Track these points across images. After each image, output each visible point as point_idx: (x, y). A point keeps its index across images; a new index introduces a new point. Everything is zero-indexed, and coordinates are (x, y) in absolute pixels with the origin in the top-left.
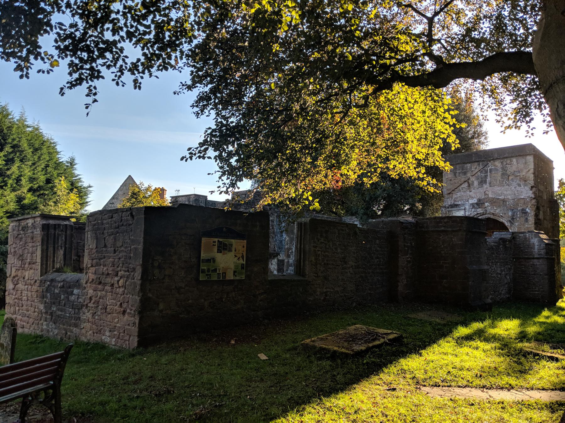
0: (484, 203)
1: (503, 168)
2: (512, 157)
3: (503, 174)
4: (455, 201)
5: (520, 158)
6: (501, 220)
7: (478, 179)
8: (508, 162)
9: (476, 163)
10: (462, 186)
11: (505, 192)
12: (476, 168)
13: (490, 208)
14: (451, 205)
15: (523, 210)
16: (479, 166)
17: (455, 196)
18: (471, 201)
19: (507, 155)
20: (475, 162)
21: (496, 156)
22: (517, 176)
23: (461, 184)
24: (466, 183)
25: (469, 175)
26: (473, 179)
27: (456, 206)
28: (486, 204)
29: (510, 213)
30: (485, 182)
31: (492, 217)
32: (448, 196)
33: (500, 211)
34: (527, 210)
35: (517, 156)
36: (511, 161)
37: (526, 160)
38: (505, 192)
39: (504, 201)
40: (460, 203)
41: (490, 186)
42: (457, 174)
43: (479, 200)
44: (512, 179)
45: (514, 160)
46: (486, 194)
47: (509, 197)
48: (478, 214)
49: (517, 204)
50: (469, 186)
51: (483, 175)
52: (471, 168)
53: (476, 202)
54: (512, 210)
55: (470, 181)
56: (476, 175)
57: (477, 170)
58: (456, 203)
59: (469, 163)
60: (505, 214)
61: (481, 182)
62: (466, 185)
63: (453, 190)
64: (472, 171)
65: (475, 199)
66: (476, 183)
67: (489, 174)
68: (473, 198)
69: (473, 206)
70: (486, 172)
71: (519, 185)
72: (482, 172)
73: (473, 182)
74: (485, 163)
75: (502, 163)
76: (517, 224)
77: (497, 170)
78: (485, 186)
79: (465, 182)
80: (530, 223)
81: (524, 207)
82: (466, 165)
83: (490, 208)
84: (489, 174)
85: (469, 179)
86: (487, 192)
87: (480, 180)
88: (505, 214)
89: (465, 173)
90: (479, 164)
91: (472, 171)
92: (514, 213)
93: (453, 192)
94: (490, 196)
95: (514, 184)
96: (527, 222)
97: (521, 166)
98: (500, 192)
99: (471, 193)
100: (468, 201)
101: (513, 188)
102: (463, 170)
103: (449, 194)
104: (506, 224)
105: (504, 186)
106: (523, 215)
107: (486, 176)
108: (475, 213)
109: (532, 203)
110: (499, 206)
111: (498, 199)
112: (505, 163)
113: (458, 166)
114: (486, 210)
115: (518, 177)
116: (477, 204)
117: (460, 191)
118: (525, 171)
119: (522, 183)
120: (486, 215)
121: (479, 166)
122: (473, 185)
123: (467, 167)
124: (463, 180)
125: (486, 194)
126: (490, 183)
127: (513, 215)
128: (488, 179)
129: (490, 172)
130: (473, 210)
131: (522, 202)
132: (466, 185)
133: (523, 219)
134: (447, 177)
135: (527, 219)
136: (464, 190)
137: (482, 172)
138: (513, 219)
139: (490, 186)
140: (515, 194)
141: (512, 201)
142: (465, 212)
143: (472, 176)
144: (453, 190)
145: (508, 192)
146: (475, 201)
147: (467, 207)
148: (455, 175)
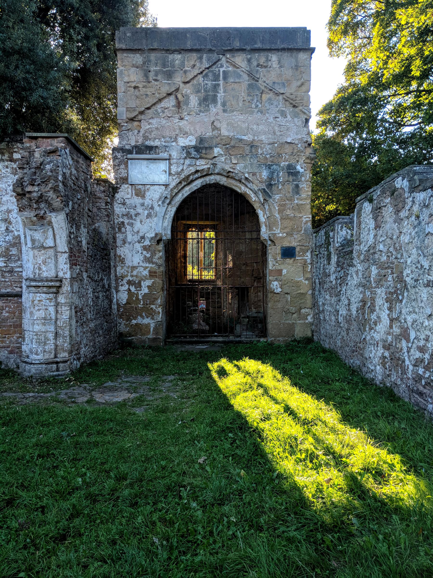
0: (211, 148)
1: (250, 74)
2: (270, 50)
3: (250, 86)
4: (146, 138)
5: (286, 55)
6: (242, 189)
7: (198, 91)
8: (262, 61)
9: (195, 55)
10: (163, 104)
11: (255, 127)
12: (194, 66)
13: (223, 159)
14: (136, 147)
15: (290, 167)
16: (201, 63)
17: (145, 126)
18: (183, 142)
19: (259, 45)
20: (191, 50)
21: (237, 44)
22: (277, 94)
23: (160, 100)
24: (172, 98)
25: (178, 79)
26: (187, 90)
27: (150, 149)
28: (217, 151)
29: (265, 174)
30: (214, 100)
31: (223, 181)
32: (130, 126)
33: (245, 167)
34: (299, 168)
35: (278, 50)
36: (268, 60)
37: (297, 61)
38: (255, 127)
39: (252, 145)
40: (157, 143)
41: (225, 111)
42: (151, 75)
43: (201, 140)
44: (270, 99)
45: (274, 58)
46: (215, 128)
47: (263, 137)
48: (197, 171)
49: (279, 155)
50: (178, 105)
51: (209, 83)
52: (183, 64)
53: (193, 143)
54: (269, 167)
55: (179, 96)
56: (195, 82)
57: (196, 71)
58: (148, 143)
59: (179, 51)
60: (254, 174)
61: (205, 99)
62: (170, 102)
63: (142, 113)
64: (185, 72)
65: (191, 137)
66: (194, 101)
67: (221, 82)
68: (186, 134)
69: (188, 153)
70: (216, 77)
71: (283, 114)
72: (206, 75)
73: (187, 97)
74: (215, 56)
75: (249, 61)
76: (277, 197)
77: (239, 76)
78: (213, 110)
79: (169, 94)
80: (304, 196)
81: (293, 162)
82: (171, 57)
83: (223, 159)
84: (221, 82)
85: (177, 90)
86: (216, 124)
87: (202, 94)
88: (254, 174)
89: (169, 75)
90: (201, 58)
91: (185, 72)
92: (273, 173)
93: (142, 117)
94: (225, 132)
95: (274, 110)
96: (298, 193)
97: (288, 73)
98: (244, 126)
99: (182, 123)
100: (176, 140)
101: (271, 120)
102: (164, 66)
103: (132, 120)
104: (253, 198)
105: (252, 113)
106: (291, 178)
107: (216, 87)
108: (193, 169)
109: (307, 154)
110: (243, 157)
111: (241, 140)
112: (255, 63)
113: (153, 56)
114: (214, 165)
115: (281, 97)
116: (197, 148)
117: (157, 114)
118: (295, 84)
119: (289, 110)
120: (212, 177)
121: (201, 63)
122: (187, 103)
123: (174, 60)
124: (165, 89)
125: (215, 128)
126: (224, 104)
127: (271, 178)
128: (221, 95)
129: (225, 78)
130: (188, 162)
131: (288, 149)
132: (170, 102)
133: (290, 187)
134: (126, 79)
135: (297, 186)
136: (167, 113)
137: (206, 75)
138: (270, 186)
139: (225, 111)
140: (274, 133)
141: (268, 147)
142: (170, 164)
143: (185, 83)
144: (142, 113)
145: (261, 127)
146: (191, 141)
147: (174, 154)
148: (146, 76)
